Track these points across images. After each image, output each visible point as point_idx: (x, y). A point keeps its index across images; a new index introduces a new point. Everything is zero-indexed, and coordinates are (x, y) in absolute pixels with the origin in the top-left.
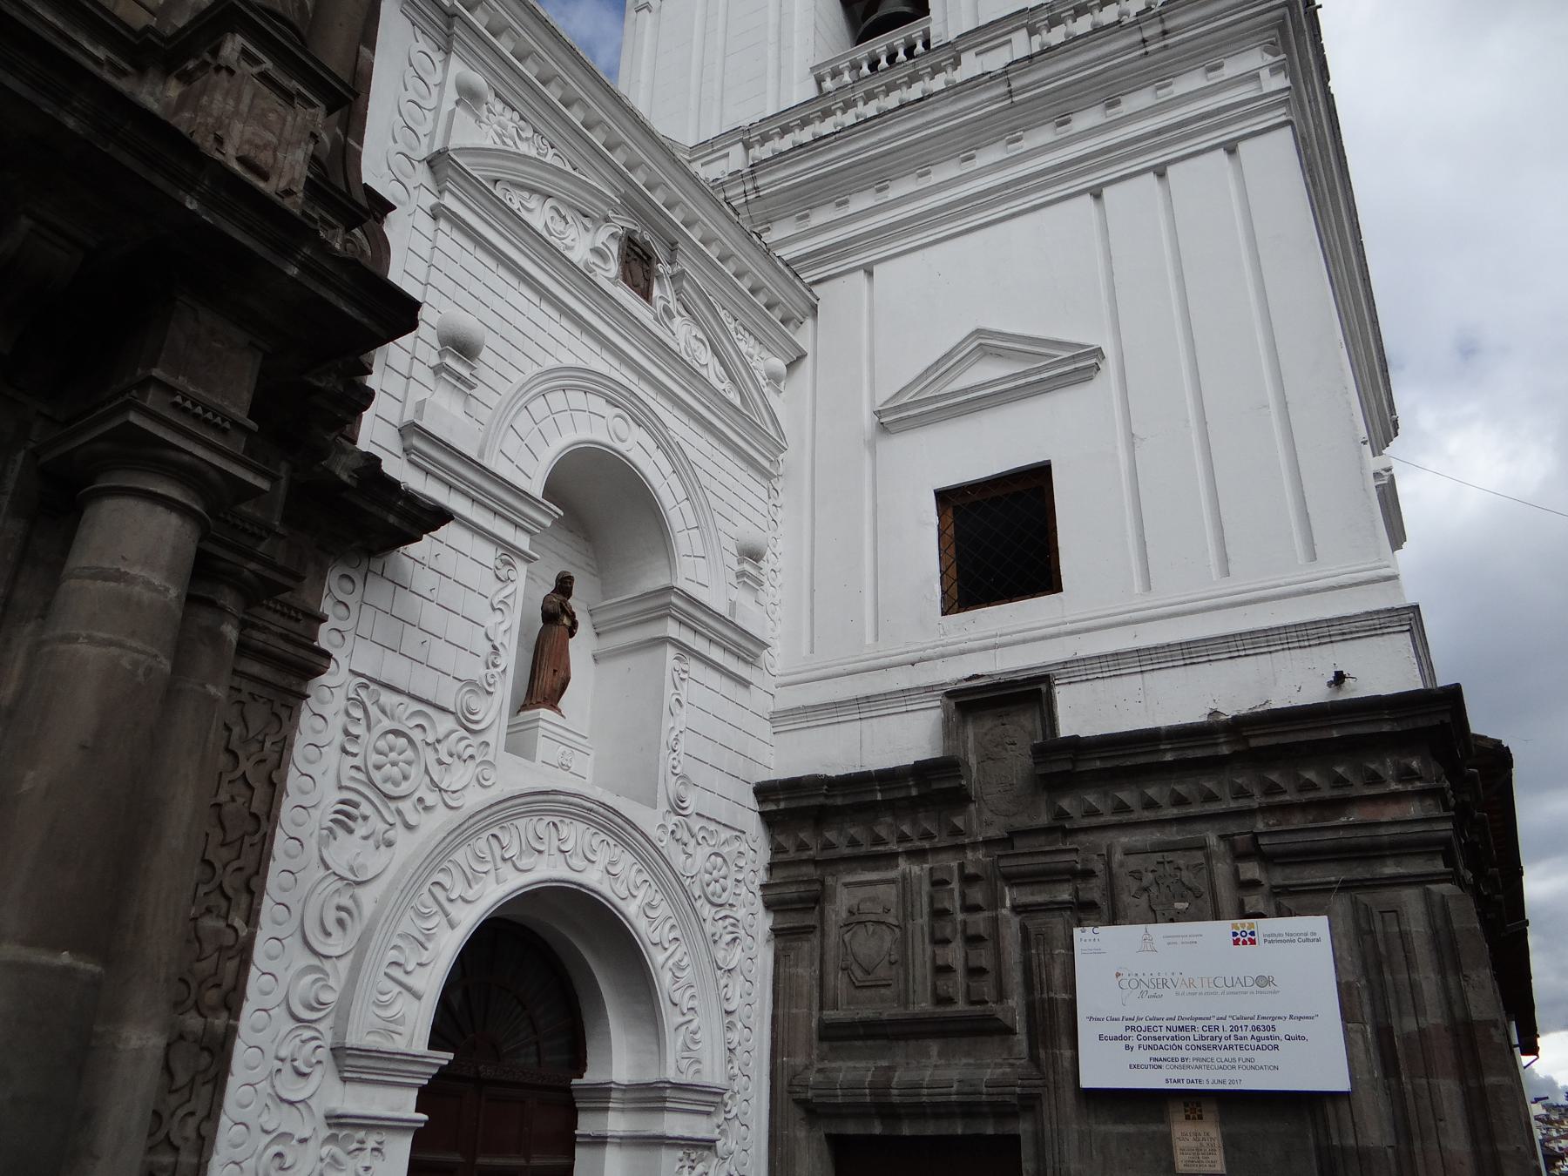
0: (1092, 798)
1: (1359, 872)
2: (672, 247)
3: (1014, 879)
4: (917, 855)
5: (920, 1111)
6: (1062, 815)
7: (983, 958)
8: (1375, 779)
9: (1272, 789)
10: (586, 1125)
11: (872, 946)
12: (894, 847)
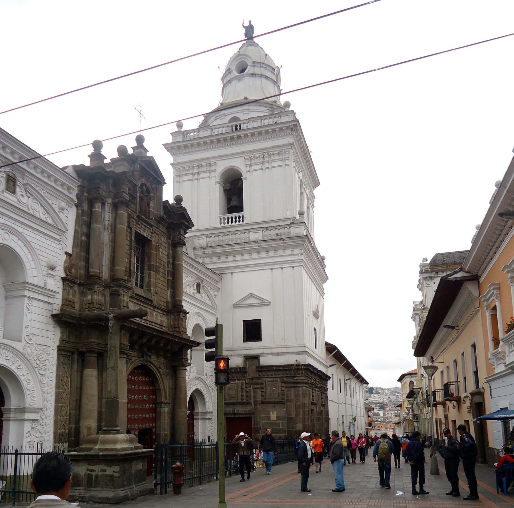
0: (264, 373)
1: (295, 385)
2: (203, 281)
3: (253, 384)
4: (239, 380)
5: (239, 414)
6: (259, 375)
7: (248, 395)
8: (299, 374)
9: (287, 374)
10: (195, 417)
11: (232, 392)
12: (235, 378)
